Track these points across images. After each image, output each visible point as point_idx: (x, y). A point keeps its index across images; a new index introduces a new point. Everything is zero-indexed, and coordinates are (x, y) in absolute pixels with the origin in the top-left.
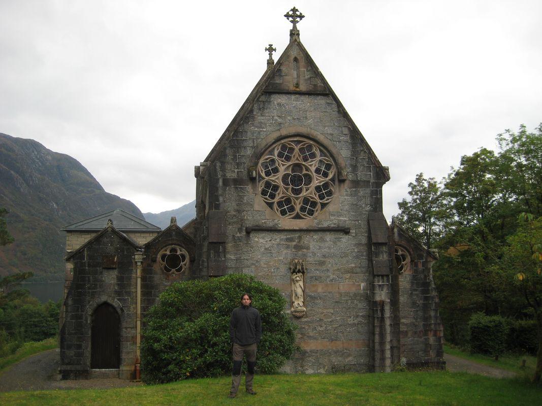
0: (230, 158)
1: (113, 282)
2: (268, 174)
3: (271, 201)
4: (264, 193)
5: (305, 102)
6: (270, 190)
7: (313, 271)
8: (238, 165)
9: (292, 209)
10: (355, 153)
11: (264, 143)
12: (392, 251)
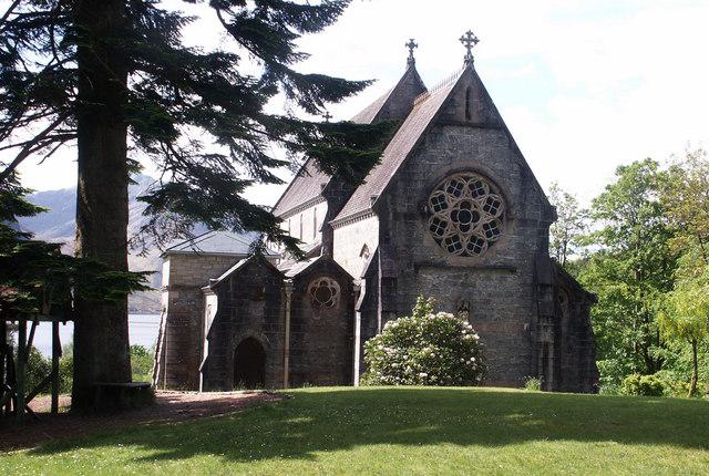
2: (437, 209)
3: (440, 237)
4: (433, 229)
6: (437, 227)
8: (409, 198)
9: (459, 246)
10: (524, 191)
11: (435, 177)
12: (555, 294)
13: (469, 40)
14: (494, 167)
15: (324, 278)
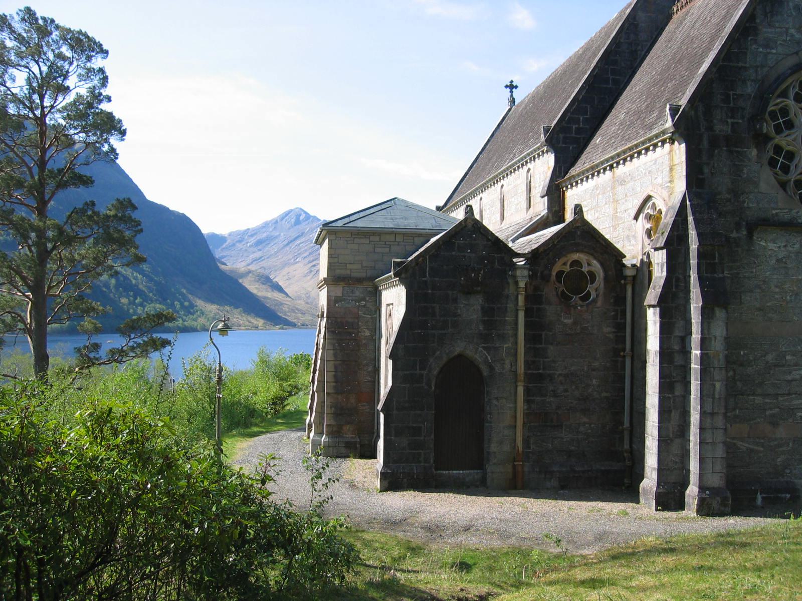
1: (475, 316)
2: (778, 130)
3: (784, 178)
15: (576, 256)
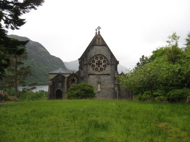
0: (85, 60)
2: (93, 63)
4: (92, 67)
5: (101, 48)
6: (93, 66)
7: (102, 83)
9: (98, 70)
10: (111, 58)
13: (99, 28)
14: (105, 53)
